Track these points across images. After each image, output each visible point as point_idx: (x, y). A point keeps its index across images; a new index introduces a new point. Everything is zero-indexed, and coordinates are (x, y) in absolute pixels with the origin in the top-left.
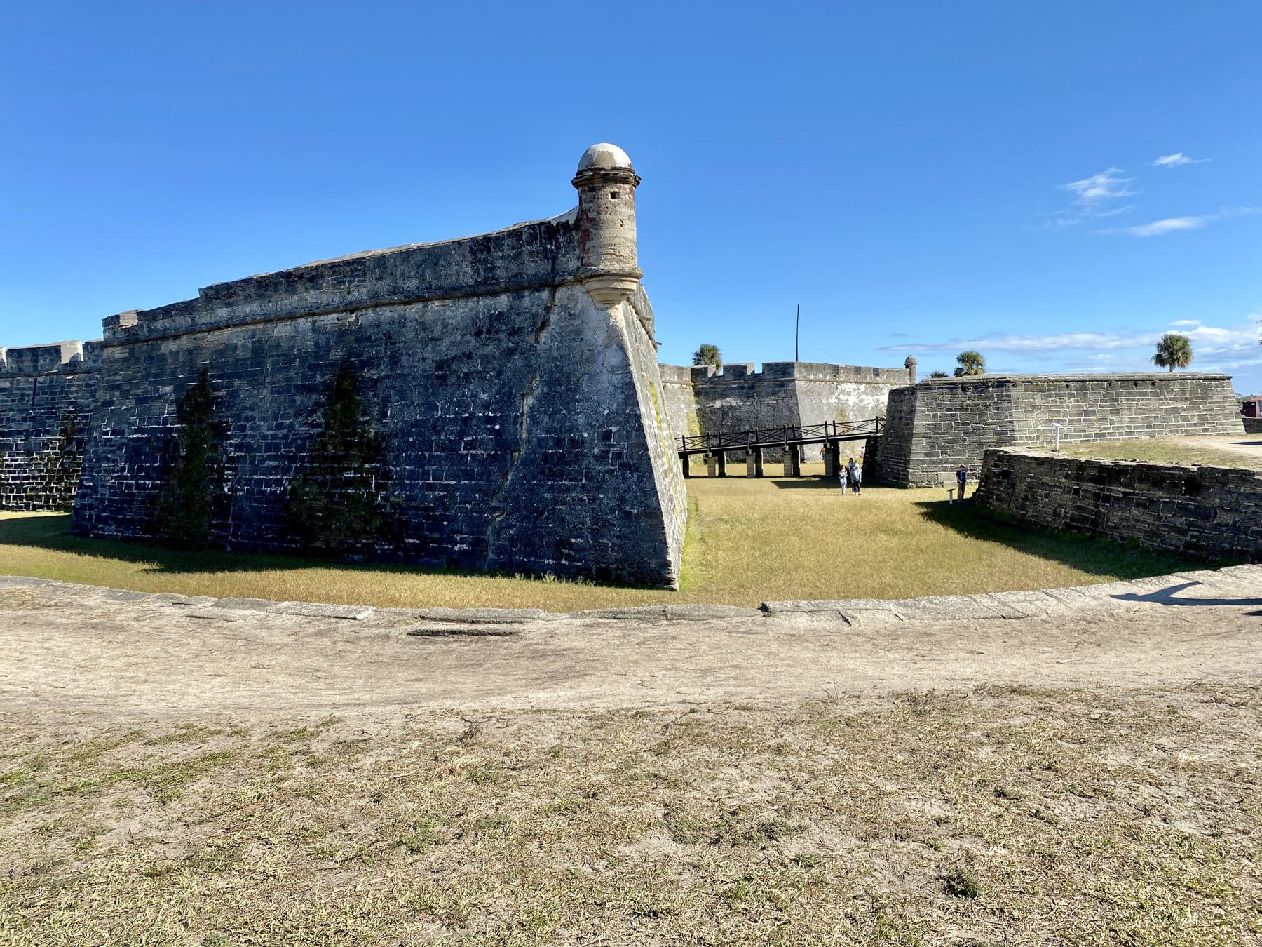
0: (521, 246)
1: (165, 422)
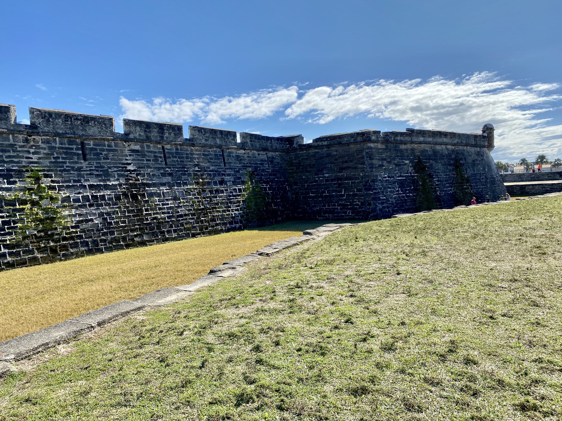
1: (411, 173)
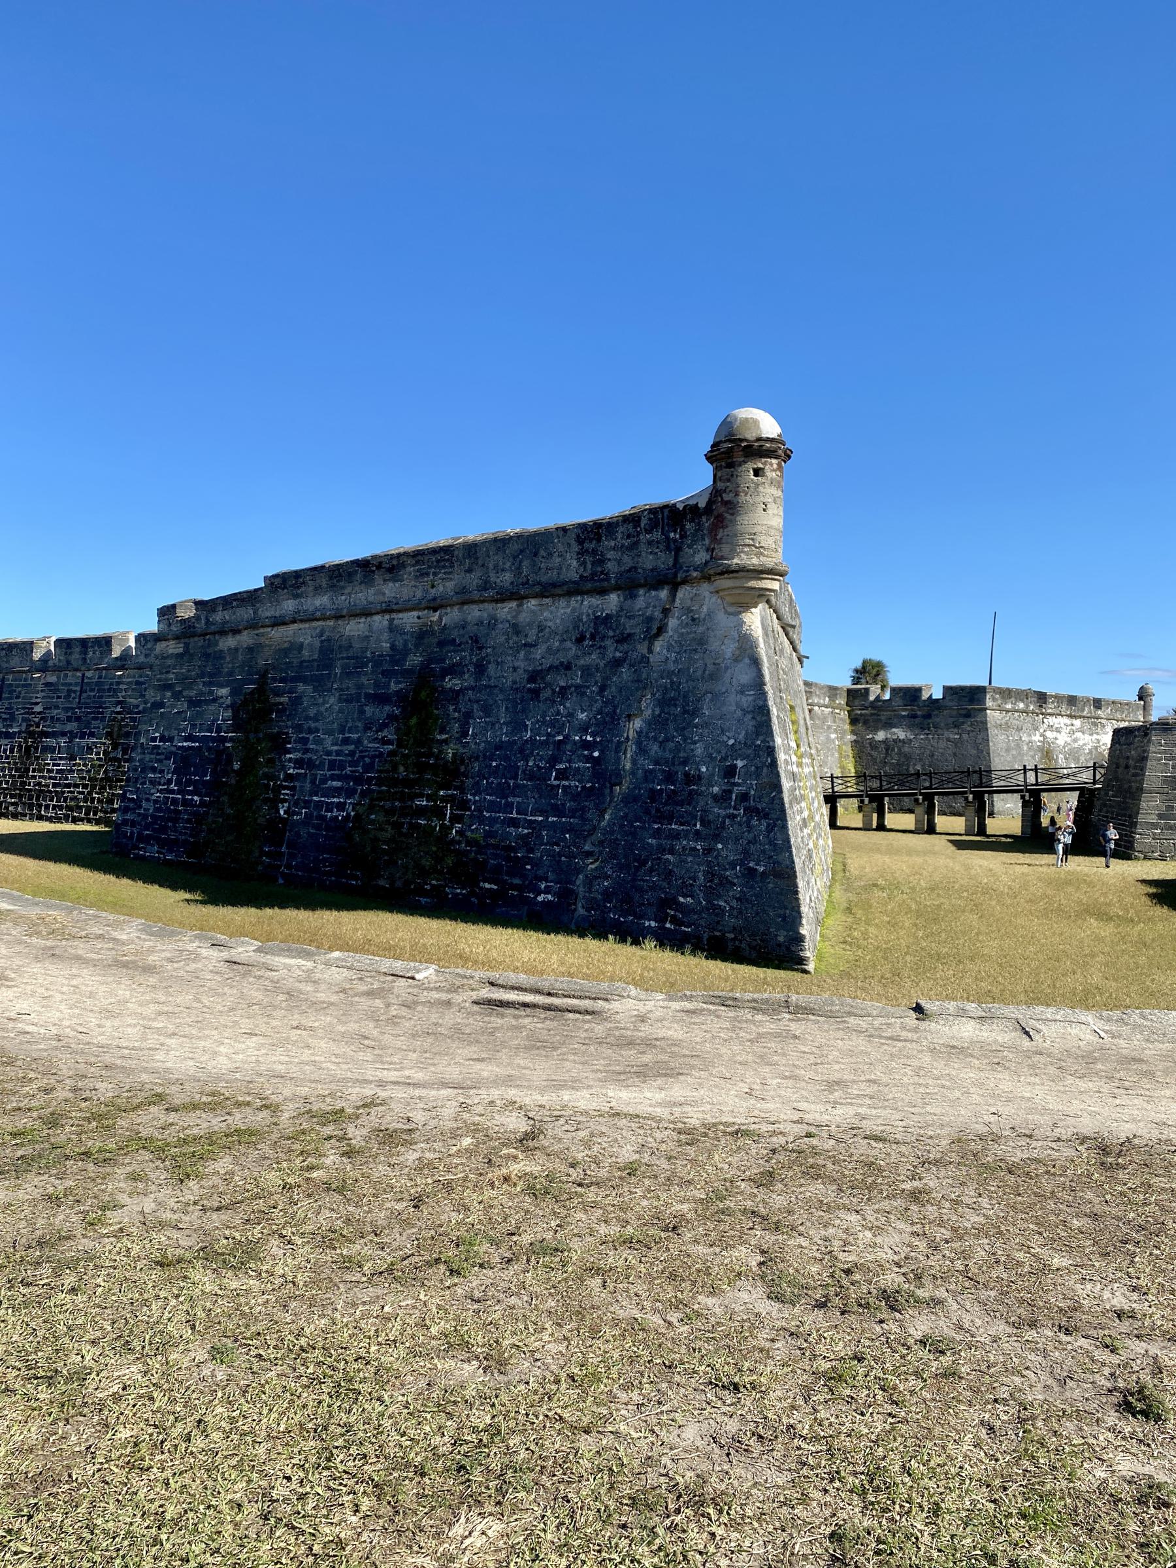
0: (638, 534)
1: (218, 731)
